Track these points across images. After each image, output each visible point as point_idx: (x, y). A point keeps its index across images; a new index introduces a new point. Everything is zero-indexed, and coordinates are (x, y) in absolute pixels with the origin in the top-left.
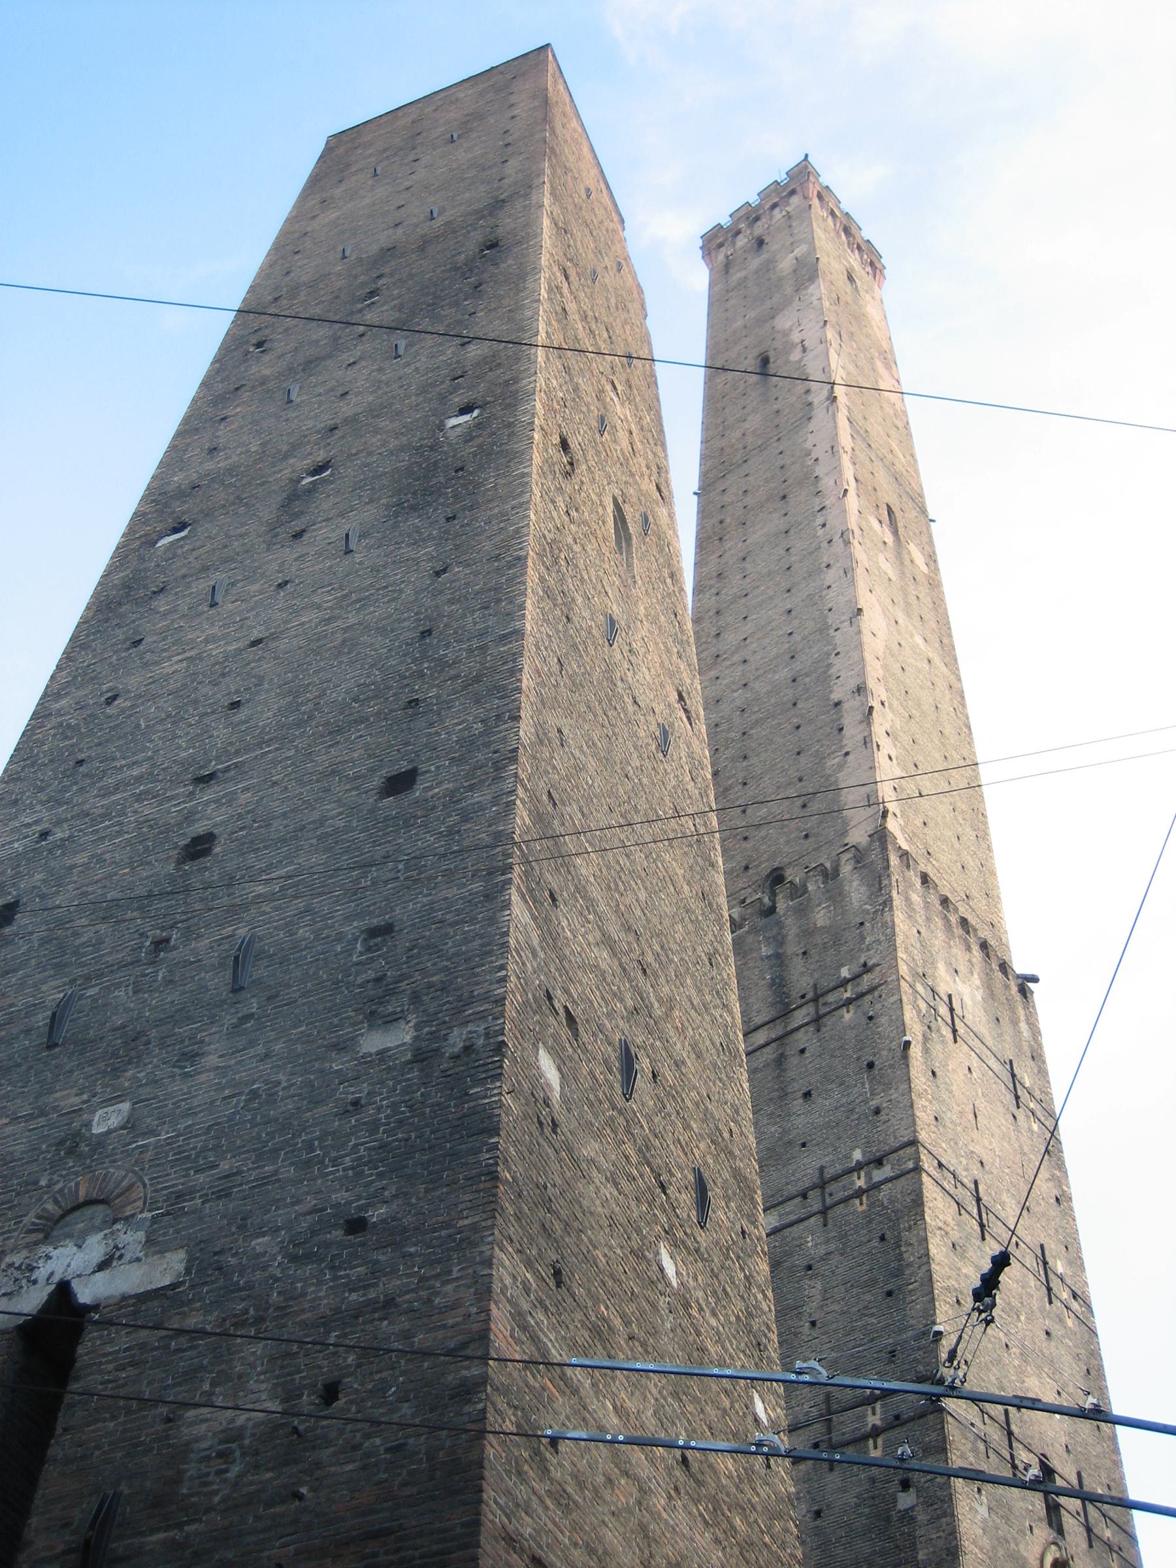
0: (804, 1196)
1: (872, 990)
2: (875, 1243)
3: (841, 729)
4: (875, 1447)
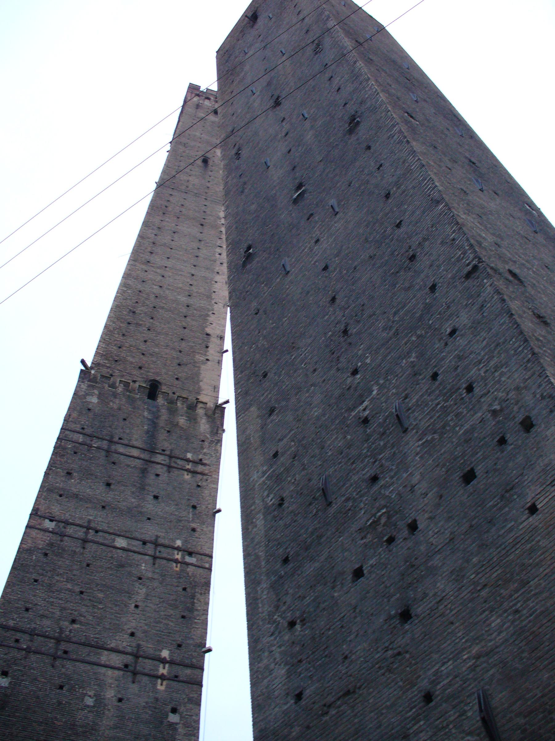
0: (144, 543)
1: (202, 474)
2: (180, 589)
3: (207, 347)
4: (162, 685)
